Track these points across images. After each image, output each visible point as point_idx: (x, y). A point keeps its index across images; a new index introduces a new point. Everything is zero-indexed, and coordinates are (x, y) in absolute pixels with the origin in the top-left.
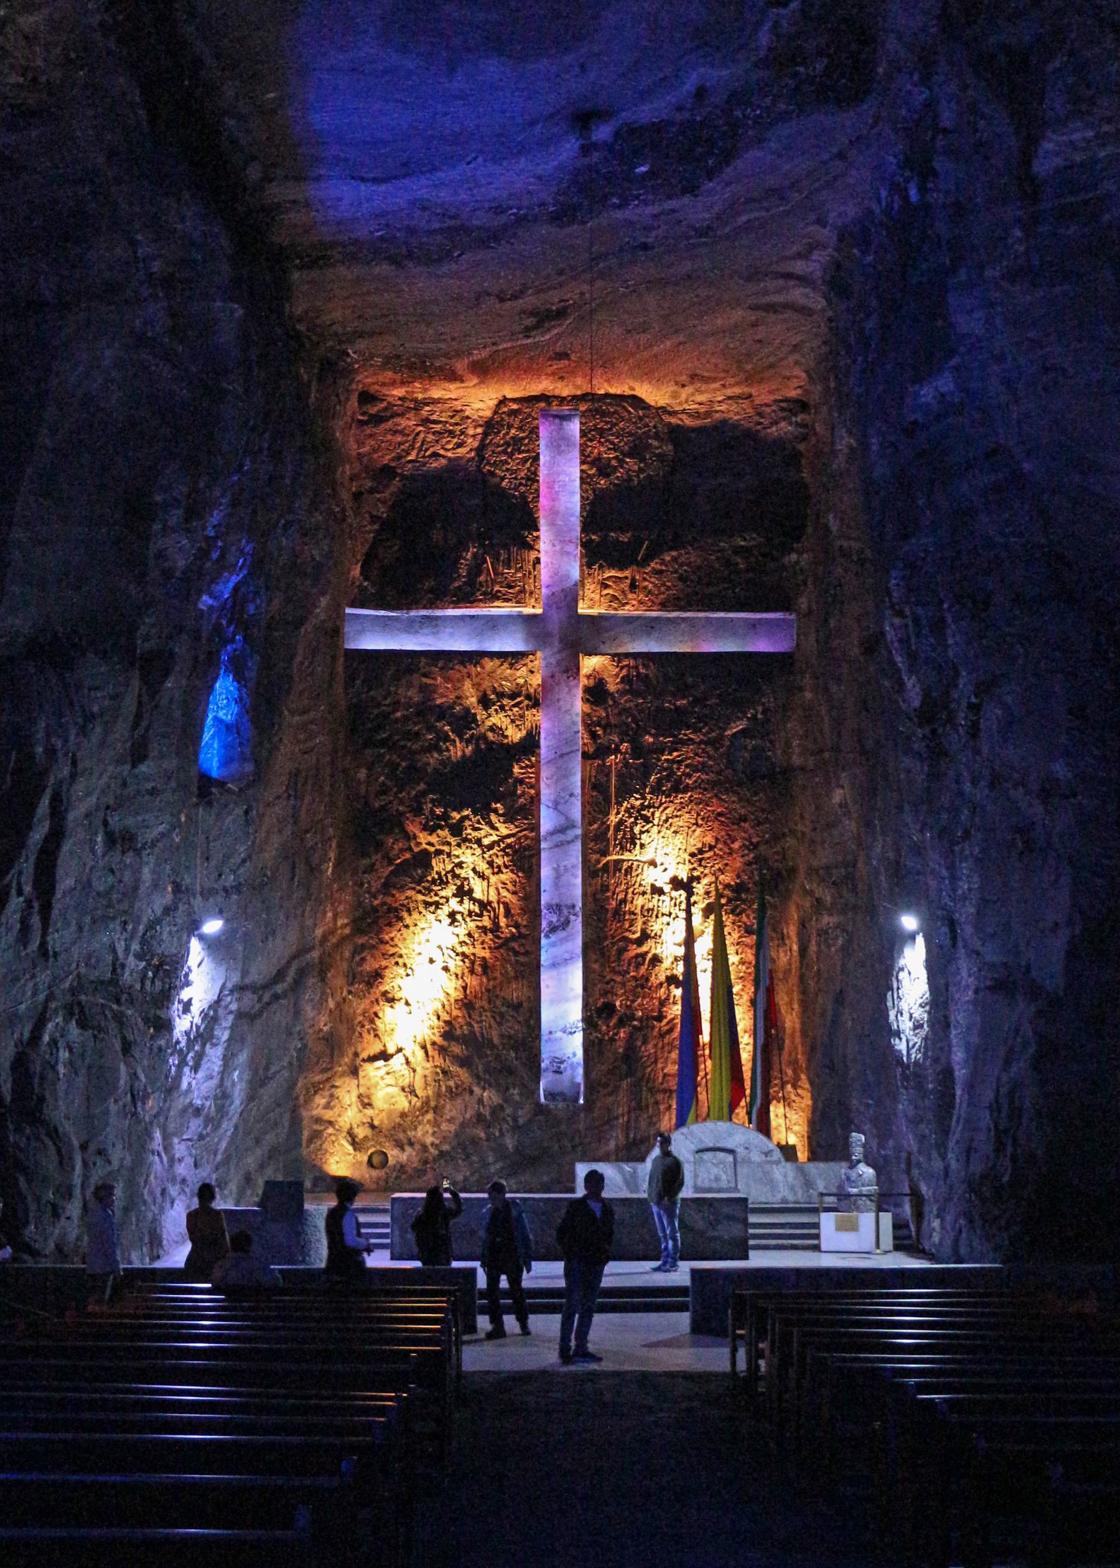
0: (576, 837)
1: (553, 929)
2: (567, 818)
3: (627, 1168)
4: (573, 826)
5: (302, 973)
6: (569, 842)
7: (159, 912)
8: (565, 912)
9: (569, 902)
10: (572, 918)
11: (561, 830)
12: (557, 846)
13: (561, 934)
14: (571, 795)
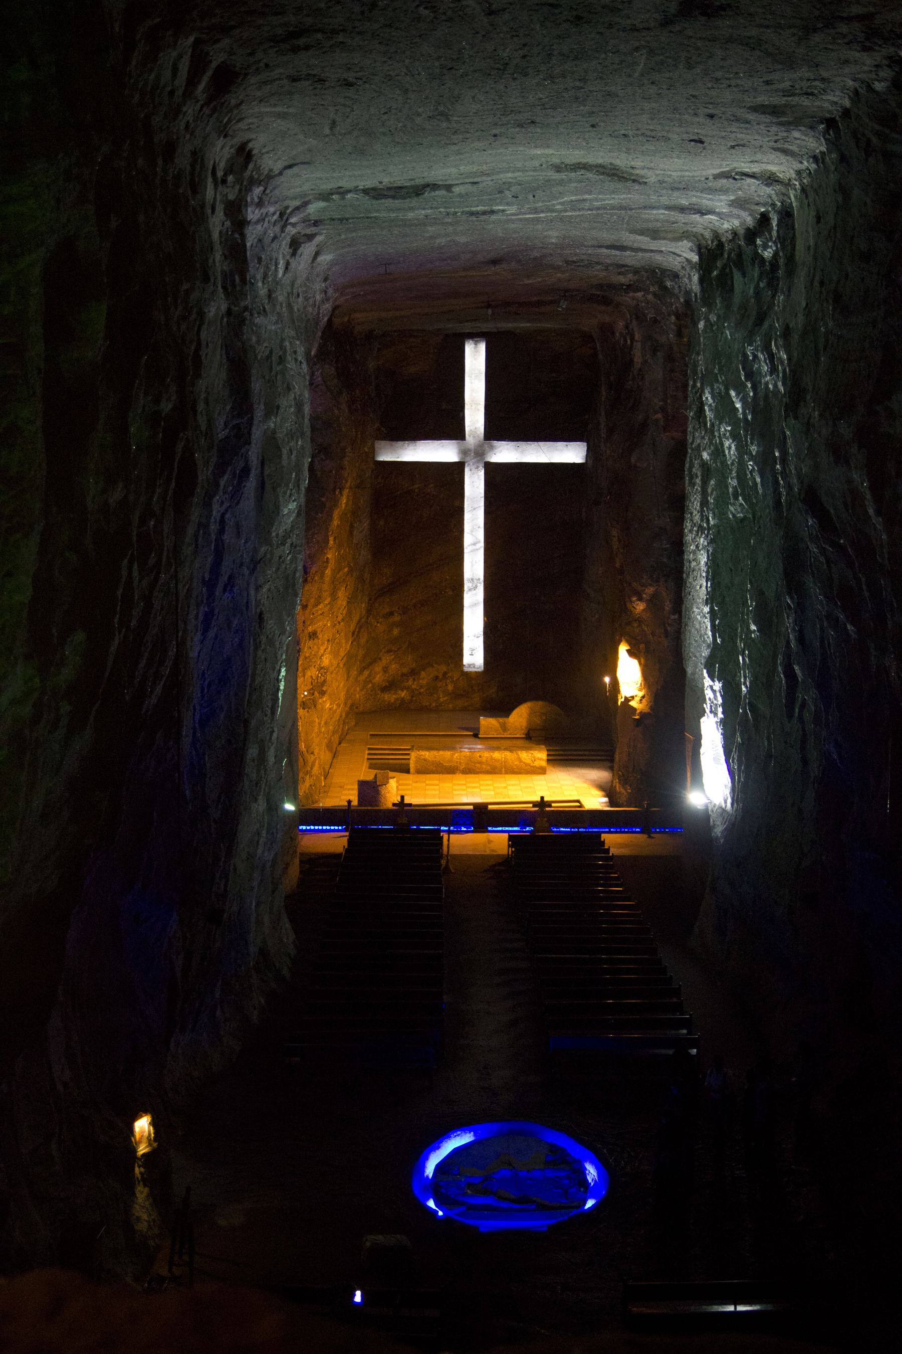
0: (481, 547)
1: (470, 590)
2: (477, 539)
3: (501, 720)
4: (479, 542)
5: (361, 628)
6: (477, 550)
7: (322, 652)
8: (475, 582)
9: (477, 578)
10: (478, 585)
11: (474, 544)
12: (472, 551)
13: (473, 592)
14: (479, 527)
